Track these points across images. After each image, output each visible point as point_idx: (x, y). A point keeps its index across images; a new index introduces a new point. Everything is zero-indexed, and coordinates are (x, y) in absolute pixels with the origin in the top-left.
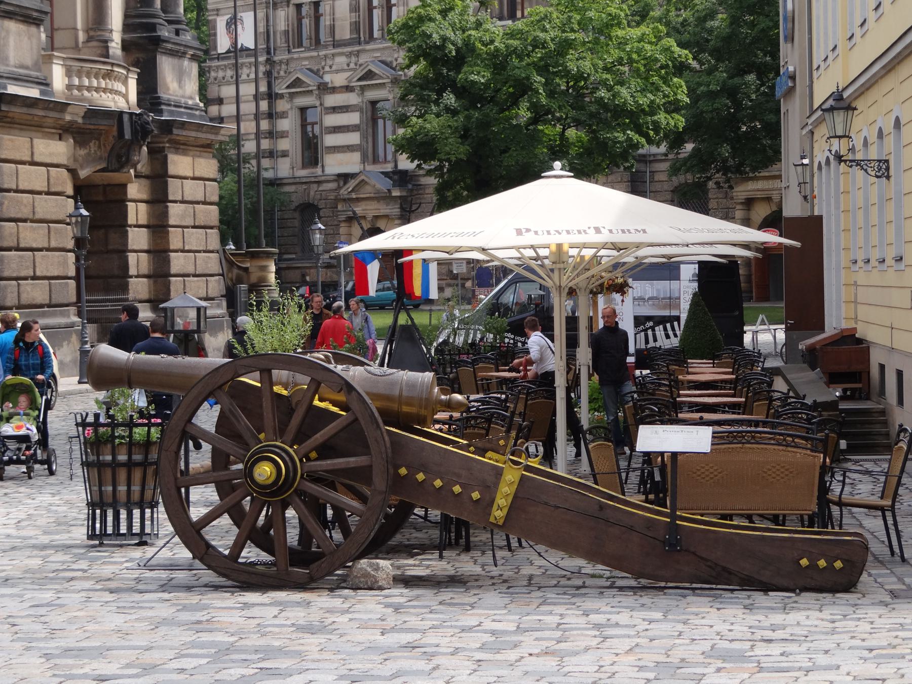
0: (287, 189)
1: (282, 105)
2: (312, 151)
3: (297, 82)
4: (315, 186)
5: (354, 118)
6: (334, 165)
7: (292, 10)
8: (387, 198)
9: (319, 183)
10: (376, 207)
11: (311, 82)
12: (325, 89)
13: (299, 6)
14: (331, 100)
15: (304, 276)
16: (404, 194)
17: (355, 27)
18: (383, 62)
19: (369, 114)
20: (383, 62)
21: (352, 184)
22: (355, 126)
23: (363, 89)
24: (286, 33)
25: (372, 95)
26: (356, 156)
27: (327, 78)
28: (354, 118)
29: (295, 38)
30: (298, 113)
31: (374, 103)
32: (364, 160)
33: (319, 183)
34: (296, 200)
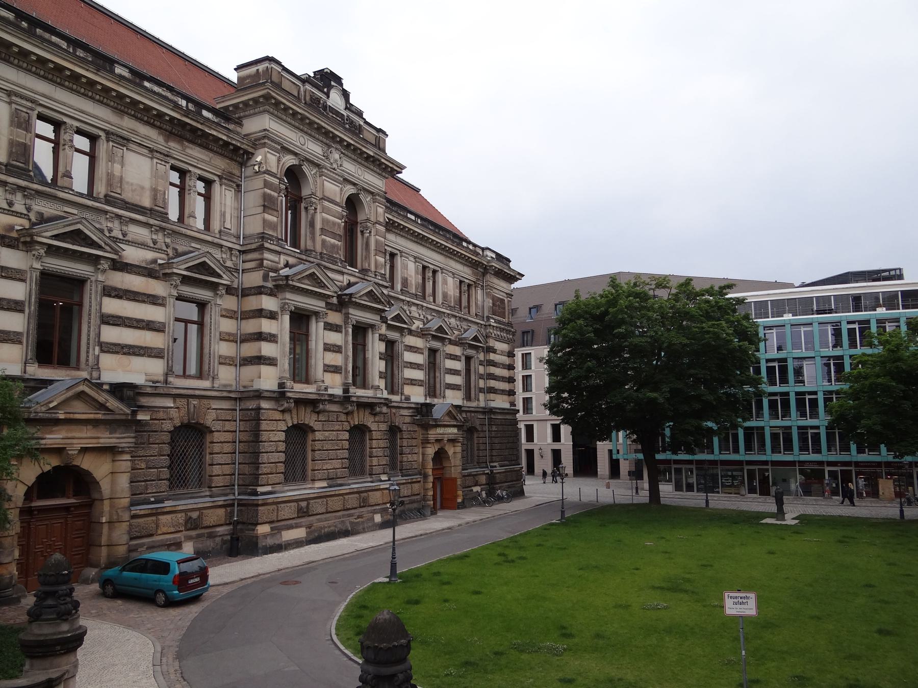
10: (89, 435)
22: (17, 302)
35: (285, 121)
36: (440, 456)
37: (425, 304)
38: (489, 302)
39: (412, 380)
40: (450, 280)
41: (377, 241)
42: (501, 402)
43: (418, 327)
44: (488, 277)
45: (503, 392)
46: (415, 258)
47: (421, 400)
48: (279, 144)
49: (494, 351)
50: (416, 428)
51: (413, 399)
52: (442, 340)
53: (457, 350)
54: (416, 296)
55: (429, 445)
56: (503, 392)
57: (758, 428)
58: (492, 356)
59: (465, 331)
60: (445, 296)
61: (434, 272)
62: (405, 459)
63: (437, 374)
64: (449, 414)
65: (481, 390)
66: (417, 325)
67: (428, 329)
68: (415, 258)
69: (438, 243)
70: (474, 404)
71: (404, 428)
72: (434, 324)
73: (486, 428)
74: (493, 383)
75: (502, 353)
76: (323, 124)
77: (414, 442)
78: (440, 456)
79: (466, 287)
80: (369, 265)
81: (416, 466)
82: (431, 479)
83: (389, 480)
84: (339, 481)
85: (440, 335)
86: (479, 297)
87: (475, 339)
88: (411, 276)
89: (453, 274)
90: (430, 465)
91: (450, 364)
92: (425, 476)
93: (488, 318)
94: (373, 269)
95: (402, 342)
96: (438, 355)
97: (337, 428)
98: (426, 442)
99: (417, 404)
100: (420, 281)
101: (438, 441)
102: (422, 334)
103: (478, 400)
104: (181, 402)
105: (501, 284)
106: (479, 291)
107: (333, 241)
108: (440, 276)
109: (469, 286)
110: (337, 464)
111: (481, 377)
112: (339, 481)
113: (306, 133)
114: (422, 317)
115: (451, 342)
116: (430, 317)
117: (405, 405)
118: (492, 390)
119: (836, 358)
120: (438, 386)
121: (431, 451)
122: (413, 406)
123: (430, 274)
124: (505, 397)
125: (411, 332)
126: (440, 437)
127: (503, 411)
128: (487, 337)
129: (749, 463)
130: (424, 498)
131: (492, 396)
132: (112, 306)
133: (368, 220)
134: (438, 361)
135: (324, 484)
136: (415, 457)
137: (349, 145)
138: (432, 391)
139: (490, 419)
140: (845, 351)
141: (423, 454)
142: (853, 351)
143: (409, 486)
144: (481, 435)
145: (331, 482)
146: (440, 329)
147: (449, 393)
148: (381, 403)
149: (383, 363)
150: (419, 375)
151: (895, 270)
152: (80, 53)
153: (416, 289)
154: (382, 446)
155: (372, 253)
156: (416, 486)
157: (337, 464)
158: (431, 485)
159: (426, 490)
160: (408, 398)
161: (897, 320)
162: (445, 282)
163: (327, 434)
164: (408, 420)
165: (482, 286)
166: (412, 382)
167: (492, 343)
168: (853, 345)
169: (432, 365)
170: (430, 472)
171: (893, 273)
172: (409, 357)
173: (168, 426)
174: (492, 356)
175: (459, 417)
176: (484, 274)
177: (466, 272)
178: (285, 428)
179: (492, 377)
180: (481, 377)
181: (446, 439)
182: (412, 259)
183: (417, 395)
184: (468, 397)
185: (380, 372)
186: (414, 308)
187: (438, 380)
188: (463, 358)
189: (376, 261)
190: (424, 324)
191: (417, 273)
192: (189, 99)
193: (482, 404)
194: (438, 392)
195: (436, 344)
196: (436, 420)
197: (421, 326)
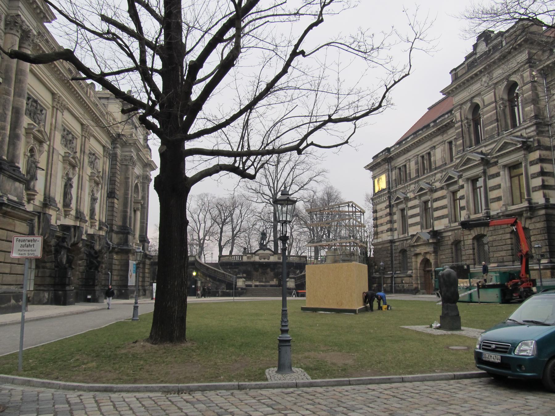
0: (397, 244)
1: (395, 209)
2: (405, 227)
3: (398, 198)
4: (405, 242)
5: (417, 210)
6: (412, 231)
7: (397, 170)
8: (427, 244)
9: (407, 240)
11: (401, 196)
12: (407, 199)
13: (400, 169)
14: (410, 204)
15: (402, 281)
16: (435, 241)
17: (417, 171)
18: (427, 183)
19: (423, 207)
20: (427, 183)
21: (415, 238)
23: (420, 196)
24: (395, 180)
25: (424, 198)
26: (419, 227)
27: (408, 195)
28: (417, 210)
29: (399, 181)
30: (400, 212)
31: (426, 202)
32: (422, 228)
33: (407, 240)
34: (400, 248)
35: (459, 92)
48: (458, 105)
76: (467, 78)
84: (506, 264)
97: (501, 232)
104: (453, 232)
107: (491, 127)
110: (503, 253)
112: (506, 264)
113: (469, 86)
132: (436, 205)
135: (496, 265)
137: (485, 68)
145: (500, 264)
152: (424, 130)
157: (503, 253)
163: (495, 237)
173: (450, 243)
178: (472, 238)
192: (447, 113)
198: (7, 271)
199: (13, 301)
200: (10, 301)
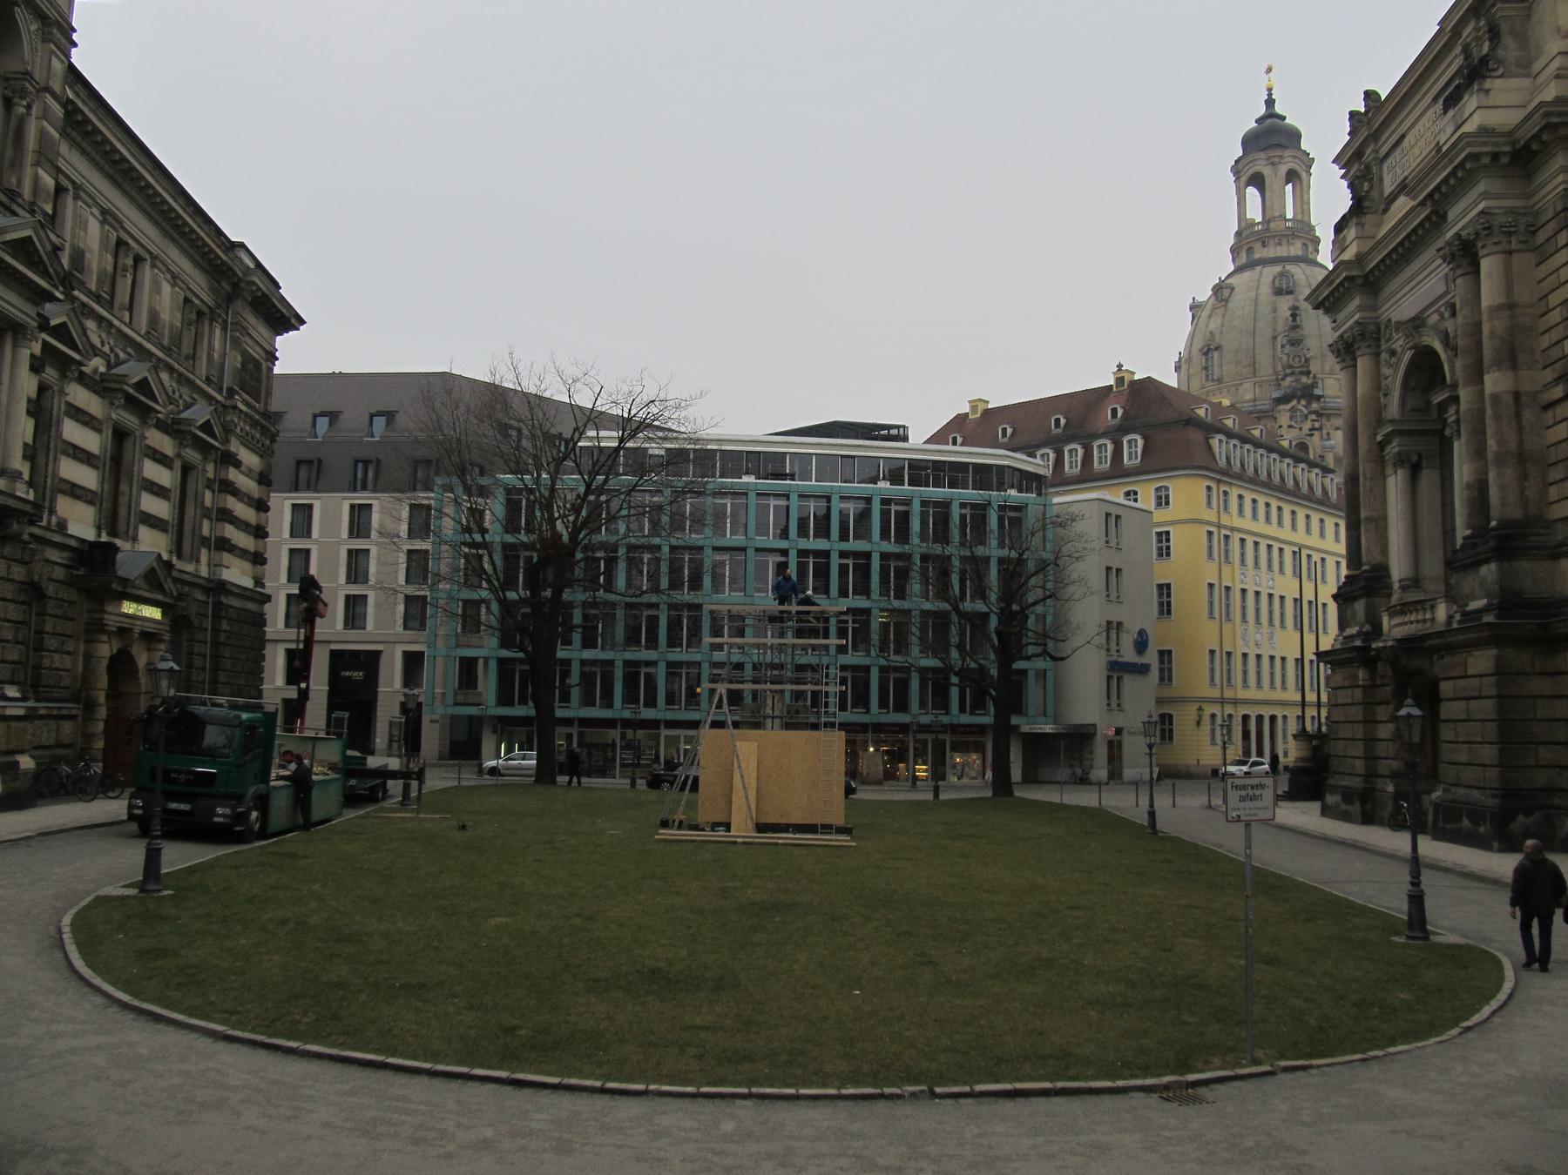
36: (121, 665)
37: (116, 322)
38: (234, 360)
39: (74, 485)
40: (166, 288)
41: (42, 133)
42: (237, 574)
43: (96, 370)
44: (238, 304)
45: (243, 553)
46: (104, 212)
47: (89, 534)
49: (237, 464)
50: (72, 595)
51: (73, 529)
52: (143, 412)
53: (165, 444)
54: (97, 298)
55: (105, 638)
56: (243, 553)
57: (689, 664)
58: (233, 474)
59: (188, 406)
60: (154, 318)
61: (138, 260)
62: (46, 662)
63: (124, 487)
64: (151, 577)
65: (205, 542)
66: (97, 364)
67: (122, 379)
68: (104, 212)
69: (157, 194)
70: (190, 568)
71: (51, 590)
72: (135, 371)
73: (208, 624)
74: (230, 532)
75: (248, 473)
77: (68, 628)
78: (121, 665)
79: (198, 316)
80: (19, 182)
81: (67, 682)
82: (102, 713)
83: (23, 699)
85: (139, 401)
86: (217, 344)
87: (206, 427)
88: (91, 251)
89: (174, 277)
90: (103, 681)
91: (152, 471)
92: (90, 706)
93: (231, 392)
94: (27, 193)
95: (62, 393)
96: (128, 444)
98: (96, 628)
99: (83, 541)
100: (110, 269)
101: (123, 632)
102: (102, 386)
103: (198, 561)
105: (259, 329)
106: (218, 332)
108: (147, 273)
109: (200, 314)
111: (207, 513)
114: (106, 349)
115: (162, 426)
116: (122, 355)
117: (57, 538)
118: (224, 545)
119: (817, 554)
120: (123, 512)
121: (105, 650)
122: (73, 543)
123: (130, 262)
124: (247, 566)
125: (82, 379)
126: (126, 623)
127: (243, 593)
128: (228, 431)
129: (671, 724)
130: (84, 754)
131: (227, 557)
133: (27, 75)
134: (127, 457)
136: (68, 662)
138: (110, 521)
139: (218, 606)
140: (833, 545)
141: (88, 657)
142: (845, 546)
143: (53, 724)
144: (199, 636)
146: (143, 386)
147: (145, 533)
148: (24, 513)
149: (31, 423)
150: (87, 477)
151: (898, 427)
153: (100, 282)
154: (14, 616)
155: (29, 159)
156: (67, 727)
158: (101, 726)
159: (89, 737)
160: (62, 526)
161: (908, 502)
162: (156, 288)
164: (59, 573)
165: (225, 322)
166: (75, 491)
167: (235, 446)
168: (844, 536)
169: (116, 464)
170: (102, 698)
171: (894, 432)
172: (73, 432)
174: (233, 474)
175: (169, 585)
176: (230, 299)
177: (199, 283)
179: (226, 516)
180: (207, 513)
181: (137, 630)
182: (96, 211)
183: (81, 523)
184: (178, 550)
185: (25, 444)
186: (91, 325)
187: (123, 500)
188: (178, 464)
189: (36, 180)
190: (109, 366)
191: (104, 244)
193: (204, 571)
194: (122, 527)
195: (129, 419)
196: (124, 581)
197: (102, 369)
198: (1463, 758)
199: (1466, 822)
200: (1461, 820)
